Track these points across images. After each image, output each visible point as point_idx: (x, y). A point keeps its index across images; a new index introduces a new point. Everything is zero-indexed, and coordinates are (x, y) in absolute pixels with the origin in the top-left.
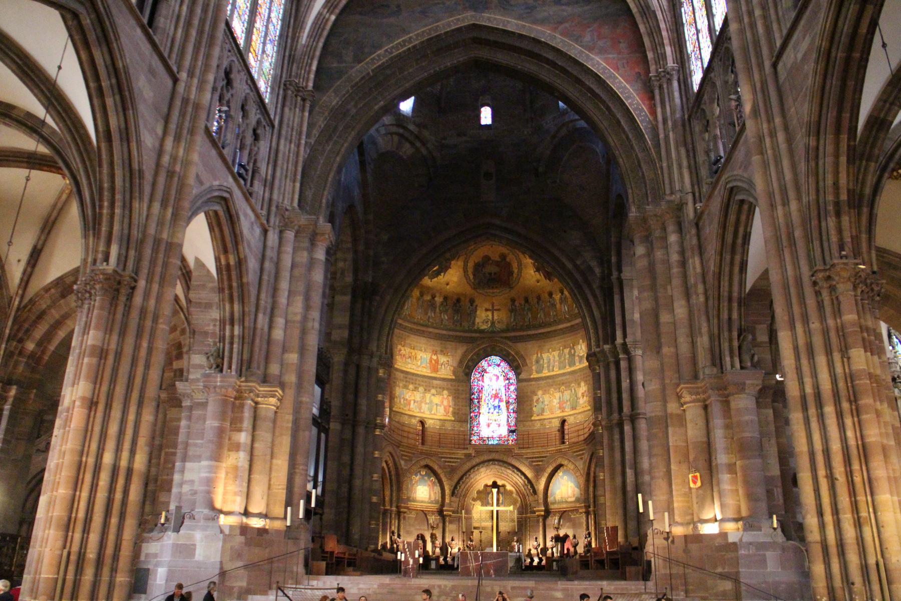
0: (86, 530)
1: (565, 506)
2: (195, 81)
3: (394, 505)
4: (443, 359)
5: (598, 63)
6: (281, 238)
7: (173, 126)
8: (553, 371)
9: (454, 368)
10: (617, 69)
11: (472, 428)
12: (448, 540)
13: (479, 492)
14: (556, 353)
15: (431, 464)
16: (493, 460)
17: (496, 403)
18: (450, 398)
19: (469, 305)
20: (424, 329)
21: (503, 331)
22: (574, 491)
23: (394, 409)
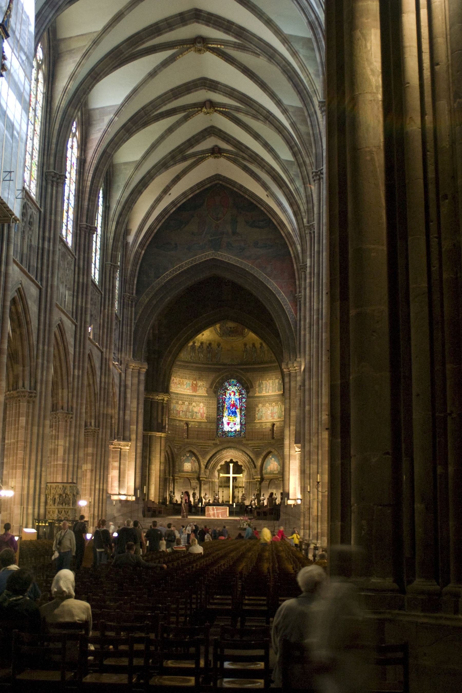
0: (94, 508)
1: (272, 476)
2: (108, 350)
3: (171, 475)
4: (200, 383)
5: (274, 285)
6: (125, 374)
7: (103, 371)
8: (268, 392)
9: (208, 389)
10: (281, 288)
11: (218, 425)
12: (202, 495)
13: (221, 466)
14: (271, 382)
15: (193, 450)
16: (230, 447)
17: (233, 410)
18: (205, 408)
19: (217, 347)
20: (188, 364)
21: (238, 365)
22: (277, 468)
23: (170, 417)
